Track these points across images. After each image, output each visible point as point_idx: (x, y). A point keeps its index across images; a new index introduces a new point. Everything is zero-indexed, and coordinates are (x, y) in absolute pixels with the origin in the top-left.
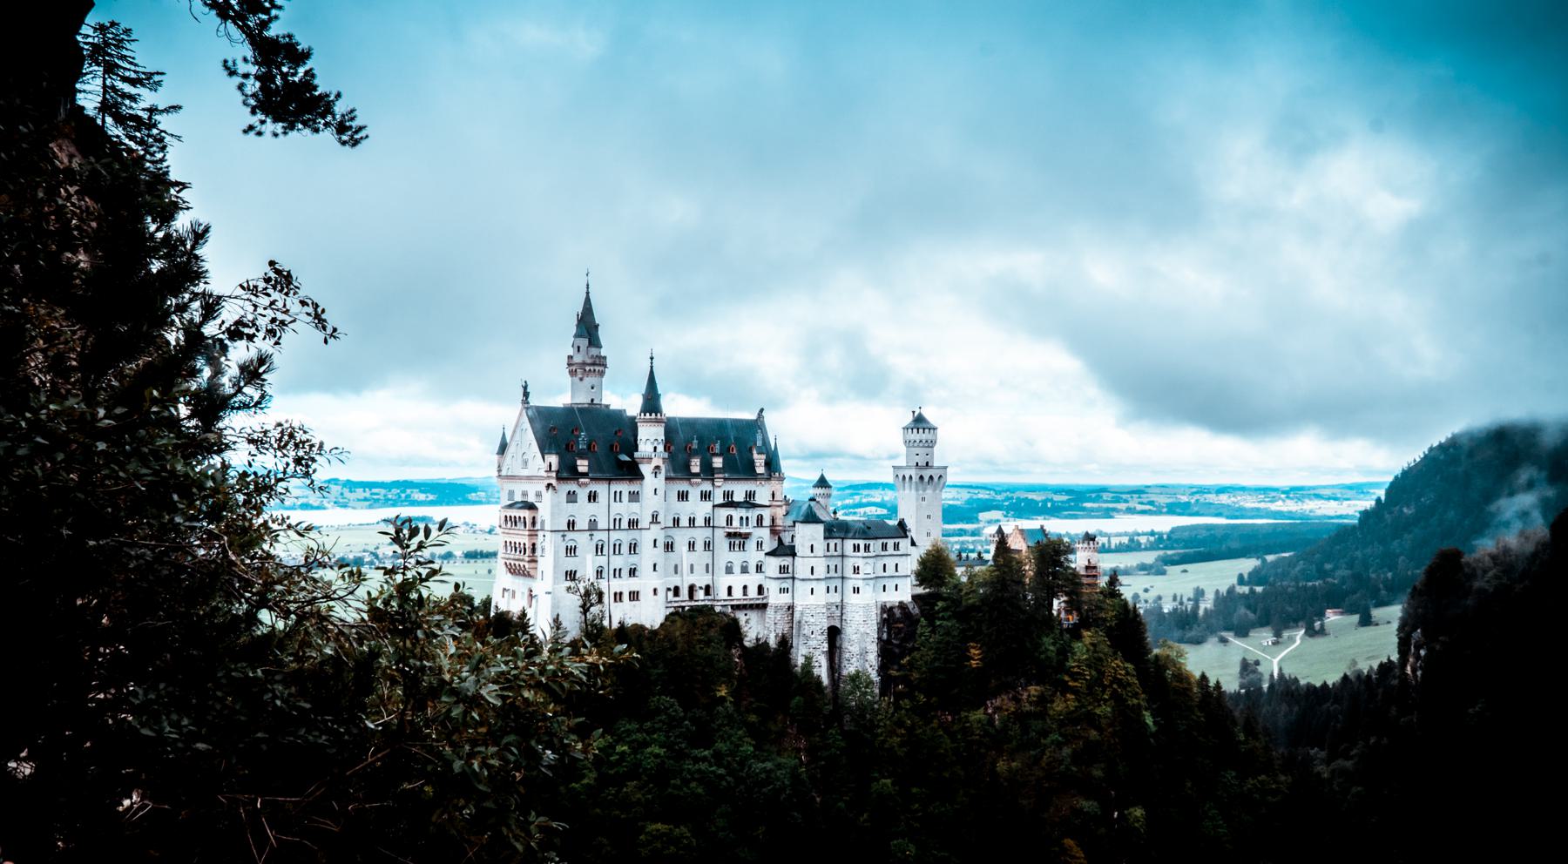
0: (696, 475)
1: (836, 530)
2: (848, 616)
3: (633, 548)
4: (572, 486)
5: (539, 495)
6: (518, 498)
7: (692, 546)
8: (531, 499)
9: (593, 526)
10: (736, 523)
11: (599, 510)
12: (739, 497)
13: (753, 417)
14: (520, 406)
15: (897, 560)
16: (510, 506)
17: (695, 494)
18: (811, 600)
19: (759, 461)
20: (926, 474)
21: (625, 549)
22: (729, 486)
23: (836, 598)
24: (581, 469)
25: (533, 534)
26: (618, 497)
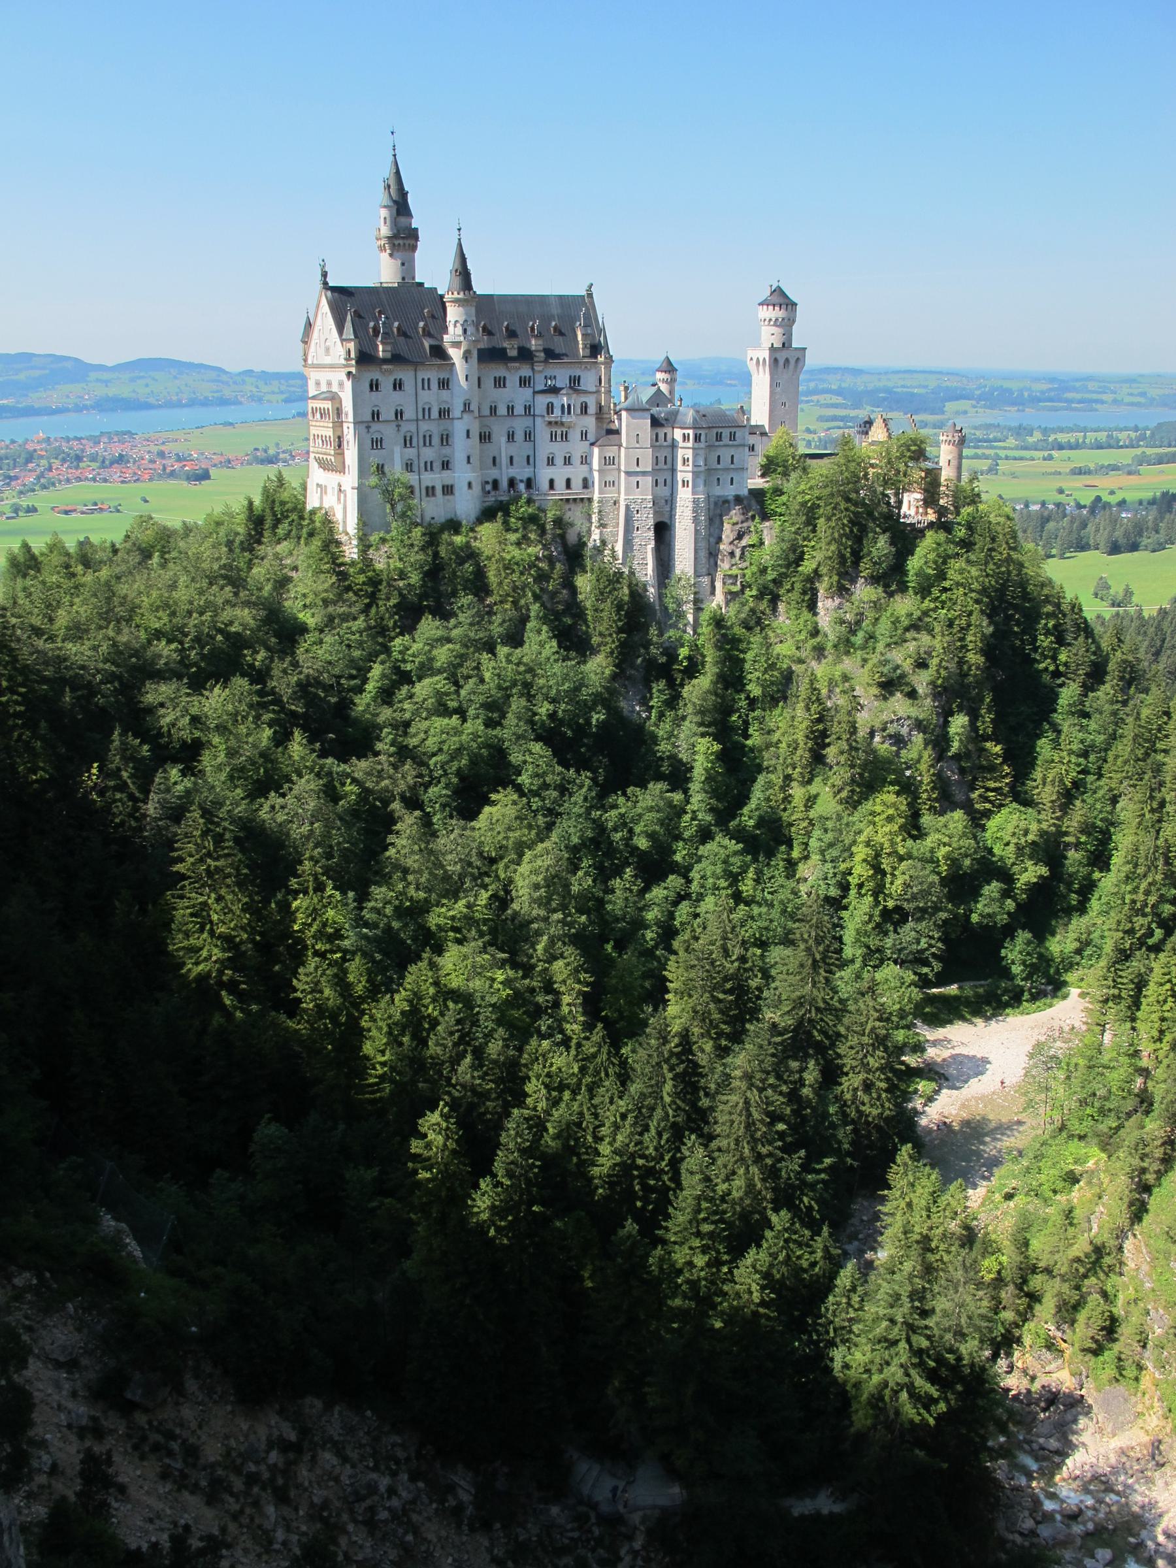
0: (513, 359)
2: (678, 511)
3: (445, 439)
4: (374, 374)
5: (341, 384)
6: (324, 388)
7: (511, 437)
8: (335, 389)
9: (399, 414)
10: (557, 412)
11: (405, 400)
12: (562, 381)
13: (584, 293)
14: (319, 285)
15: (732, 451)
16: (314, 398)
17: (513, 380)
18: (637, 496)
20: (782, 357)
21: (436, 440)
22: (550, 372)
23: (664, 492)
25: (338, 425)
26: (426, 384)
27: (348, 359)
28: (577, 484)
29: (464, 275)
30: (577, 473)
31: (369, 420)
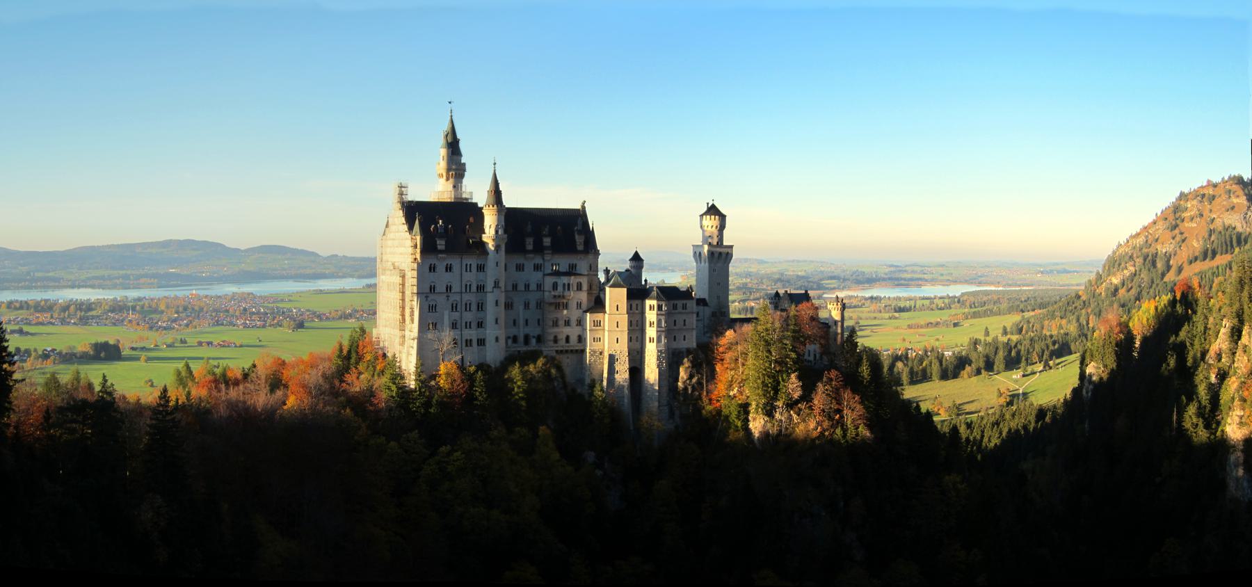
0: (530, 252)
1: (638, 293)
3: (481, 307)
4: (432, 260)
7: (527, 306)
9: (449, 288)
10: (560, 288)
11: (453, 279)
13: (579, 207)
15: (684, 317)
17: (529, 266)
19: (579, 240)
21: (474, 307)
23: (638, 346)
24: (439, 247)
26: (468, 268)
27: (416, 246)
28: (574, 339)
29: (497, 194)
30: (573, 332)
31: (427, 293)
